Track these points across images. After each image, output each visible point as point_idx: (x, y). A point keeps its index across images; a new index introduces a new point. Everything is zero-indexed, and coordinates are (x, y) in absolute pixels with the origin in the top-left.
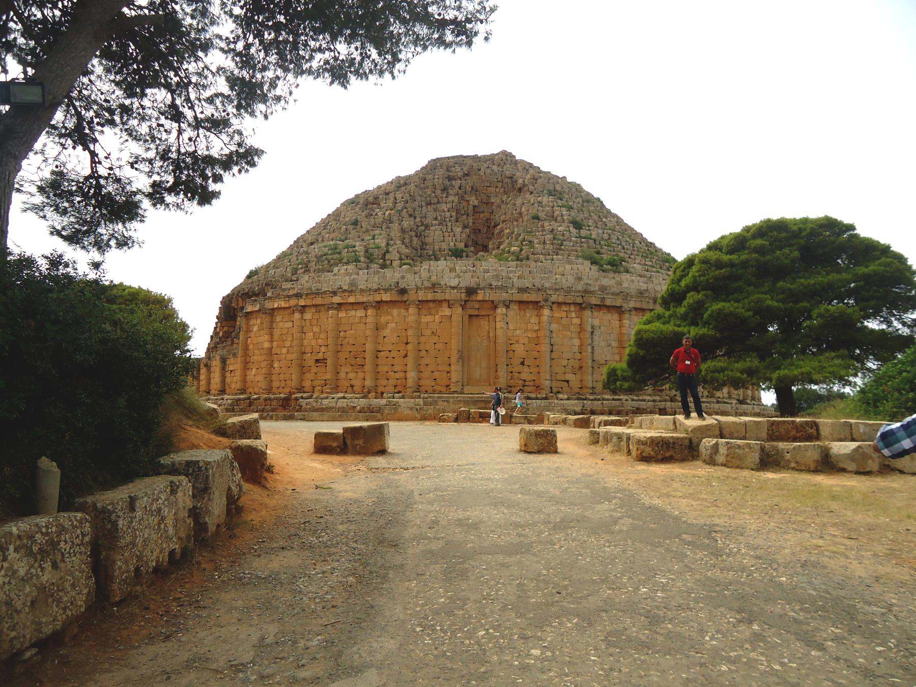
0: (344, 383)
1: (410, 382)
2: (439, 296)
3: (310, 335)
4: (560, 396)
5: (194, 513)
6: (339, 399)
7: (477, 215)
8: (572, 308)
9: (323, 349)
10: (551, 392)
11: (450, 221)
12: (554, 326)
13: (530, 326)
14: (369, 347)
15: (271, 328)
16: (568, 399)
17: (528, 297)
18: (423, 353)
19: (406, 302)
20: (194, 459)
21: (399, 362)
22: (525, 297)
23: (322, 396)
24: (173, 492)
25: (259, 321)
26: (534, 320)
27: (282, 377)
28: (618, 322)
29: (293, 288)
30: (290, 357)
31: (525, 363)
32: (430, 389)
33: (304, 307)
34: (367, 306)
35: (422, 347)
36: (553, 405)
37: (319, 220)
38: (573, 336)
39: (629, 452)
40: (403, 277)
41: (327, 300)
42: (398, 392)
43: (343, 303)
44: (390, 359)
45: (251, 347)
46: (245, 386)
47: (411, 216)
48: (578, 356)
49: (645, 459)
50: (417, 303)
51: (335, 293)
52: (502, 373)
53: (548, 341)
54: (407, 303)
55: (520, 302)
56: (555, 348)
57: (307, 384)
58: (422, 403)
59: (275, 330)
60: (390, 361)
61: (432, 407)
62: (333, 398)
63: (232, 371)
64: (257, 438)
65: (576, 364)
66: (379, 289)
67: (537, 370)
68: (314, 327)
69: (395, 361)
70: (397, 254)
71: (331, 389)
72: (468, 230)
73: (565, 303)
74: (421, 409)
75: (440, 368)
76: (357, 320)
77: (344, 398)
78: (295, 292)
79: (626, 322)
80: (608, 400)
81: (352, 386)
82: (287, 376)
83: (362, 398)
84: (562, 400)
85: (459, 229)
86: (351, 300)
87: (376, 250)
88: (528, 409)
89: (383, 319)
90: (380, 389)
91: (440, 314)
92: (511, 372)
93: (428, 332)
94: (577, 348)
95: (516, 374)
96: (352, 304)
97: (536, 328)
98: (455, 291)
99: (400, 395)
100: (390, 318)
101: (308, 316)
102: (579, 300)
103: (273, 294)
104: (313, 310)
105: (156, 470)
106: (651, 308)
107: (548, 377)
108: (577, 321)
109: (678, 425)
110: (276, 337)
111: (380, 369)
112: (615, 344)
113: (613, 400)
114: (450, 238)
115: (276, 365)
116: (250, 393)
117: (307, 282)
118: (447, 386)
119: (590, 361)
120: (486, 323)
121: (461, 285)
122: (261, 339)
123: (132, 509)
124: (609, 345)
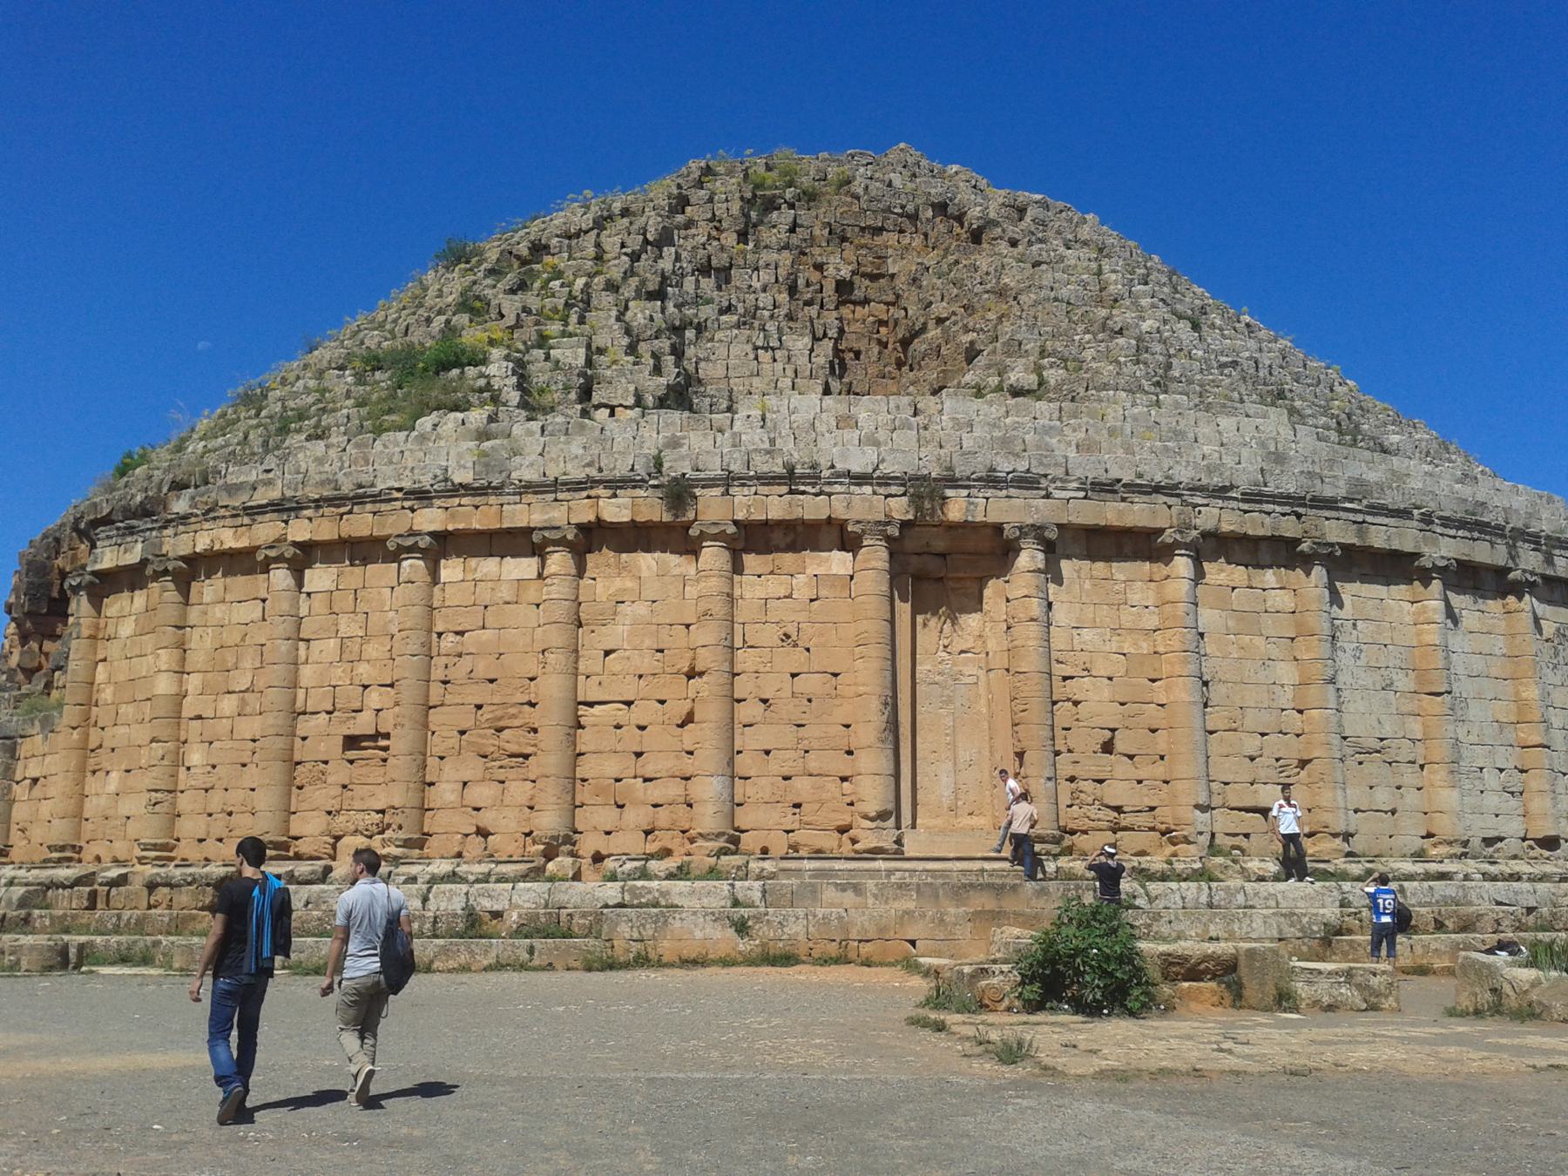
0: (448, 823)
1: (708, 818)
2: (812, 507)
7: (846, 311)
13: (1127, 617)
14: (552, 688)
17: (1120, 513)
22: (1112, 513)
27: (216, 800)
29: (269, 483)
31: (1119, 745)
32: (779, 844)
35: (742, 687)
36: (1240, 899)
38: (1275, 652)
40: (674, 443)
42: (666, 853)
44: (630, 732)
45: (107, 695)
46: (78, 836)
47: (651, 296)
50: (731, 529)
51: (421, 496)
56: (1217, 692)
61: (801, 912)
62: (413, 880)
63: (35, 781)
65: (1293, 749)
67: (1160, 770)
68: (343, 620)
69: (648, 741)
71: (407, 844)
75: (813, 761)
77: (453, 877)
78: (275, 494)
80: (1410, 877)
81: (483, 833)
82: (236, 797)
83: (524, 877)
84: (1261, 879)
90: (589, 844)
91: (810, 571)
92: (1072, 779)
93: (770, 635)
95: (1088, 786)
98: (868, 489)
100: (629, 584)
110: (196, 658)
113: (1428, 876)
114: (779, 366)
115: (196, 757)
116: (98, 859)
117: (320, 461)
118: (843, 830)
121: (886, 469)
122: (143, 666)
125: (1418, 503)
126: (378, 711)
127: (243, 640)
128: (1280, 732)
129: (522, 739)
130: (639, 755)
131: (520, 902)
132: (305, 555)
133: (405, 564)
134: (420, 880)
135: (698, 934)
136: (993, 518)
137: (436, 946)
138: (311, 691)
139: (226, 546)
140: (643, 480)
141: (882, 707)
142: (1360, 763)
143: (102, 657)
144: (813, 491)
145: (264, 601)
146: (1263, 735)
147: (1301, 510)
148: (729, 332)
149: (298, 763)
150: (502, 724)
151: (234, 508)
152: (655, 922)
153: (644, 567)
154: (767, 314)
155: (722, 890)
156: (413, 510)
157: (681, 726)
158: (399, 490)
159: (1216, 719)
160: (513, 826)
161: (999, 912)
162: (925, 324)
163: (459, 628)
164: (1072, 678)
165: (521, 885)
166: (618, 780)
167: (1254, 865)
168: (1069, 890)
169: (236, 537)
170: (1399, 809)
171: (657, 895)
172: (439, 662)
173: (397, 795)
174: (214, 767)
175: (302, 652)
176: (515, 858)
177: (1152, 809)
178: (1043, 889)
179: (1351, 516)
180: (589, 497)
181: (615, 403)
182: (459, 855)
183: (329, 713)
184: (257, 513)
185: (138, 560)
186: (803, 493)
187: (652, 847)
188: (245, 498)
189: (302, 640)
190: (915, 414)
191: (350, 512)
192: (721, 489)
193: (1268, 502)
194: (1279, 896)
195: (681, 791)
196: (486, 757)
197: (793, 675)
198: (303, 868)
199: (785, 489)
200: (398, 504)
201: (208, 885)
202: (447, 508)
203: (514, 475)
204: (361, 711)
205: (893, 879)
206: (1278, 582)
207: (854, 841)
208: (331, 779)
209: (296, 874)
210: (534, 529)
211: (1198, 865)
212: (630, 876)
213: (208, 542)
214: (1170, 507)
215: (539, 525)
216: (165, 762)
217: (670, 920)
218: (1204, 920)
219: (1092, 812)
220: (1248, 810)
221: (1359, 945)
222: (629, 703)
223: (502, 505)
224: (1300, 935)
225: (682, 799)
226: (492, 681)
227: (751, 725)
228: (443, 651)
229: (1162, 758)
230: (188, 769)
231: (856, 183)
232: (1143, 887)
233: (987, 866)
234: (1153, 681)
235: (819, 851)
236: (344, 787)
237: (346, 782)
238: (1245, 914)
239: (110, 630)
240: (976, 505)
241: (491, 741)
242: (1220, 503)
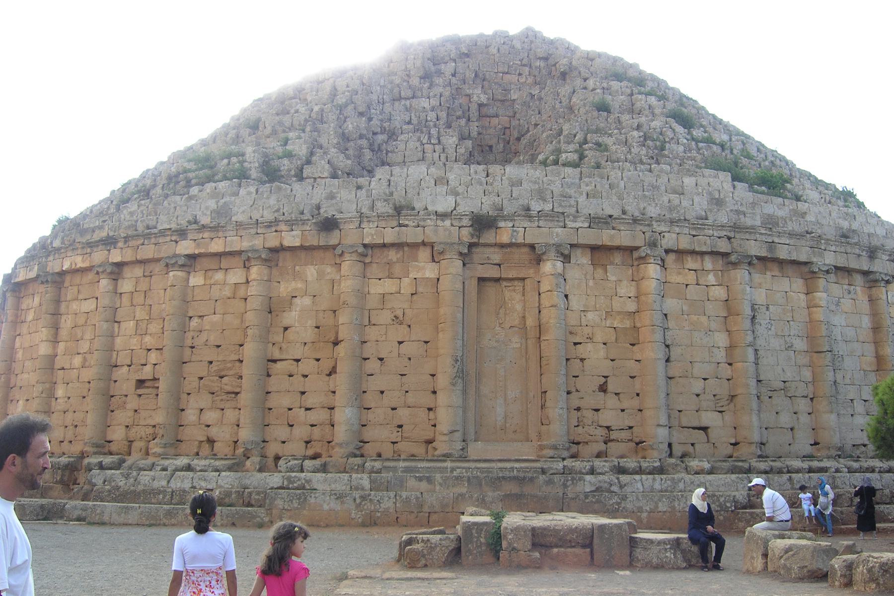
0: (193, 434)
1: (341, 433)
2: (412, 235)
3: (129, 326)
4: (694, 464)
6: (176, 470)
9: (153, 357)
10: (671, 455)
11: (435, 126)
12: (672, 304)
13: (617, 305)
14: (250, 350)
15: (56, 314)
16: (711, 472)
18: (372, 365)
19: (334, 247)
21: (317, 385)
22: (606, 237)
23: (142, 463)
25: (37, 299)
26: (626, 289)
28: (803, 297)
29: (101, 228)
30: (87, 374)
31: (610, 387)
33: (120, 265)
34: (249, 259)
35: (369, 350)
36: (681, 486)
38: (713, 326)
40: (331, 196)
41: (166, 250)
42: (315, 457)
43: (200, 255)
44: (298, 379)
45: (20, 355)
48: (727, 371)
50: (361, 250)
51: (182, 233)
52: (557, 410)
53: (658, 336)
54: (338, 251)
55: (595, 249)
56: (675, 352)
57: (117, 434)
58: (366, 483)
59: (64, 318)
60: (298, 383)
61: (392, 494)
62: (164, 469)
65: (724, 390)
66: (276, 221)
67: (636, 403)
69: (308, 385)
70: (327, 166)
72: (469, 143)
73: (693, 252)
74: (363, 498)
75: (411, 399)
76: (227, 292)
77: (189, 468)
78: (103, 234)
79: (821, 296)
80: (798, 471)
81: (211, 441)
82: (79, 416)
83: (230, 469)
85: (455, 139)
86: (216, 246)
87: (286, 161)
88: (624, 498)
89: (285, 288)
90: (273, 449)
91: (411, 276)
92: (578, 409)
93: (385, 317)
94: (723, 353)
95: (588, 414)
96: (219, 255)
97: (632, 307)
98: (447, 223)
99: (317, 462)
100: (300, 285)
101: (126, 286)
102: (723, 246)
103: (63, 243)
104: (138, 271)
106: (866, 268)
107: (663, 420)
108: (719, 293)
110: (64, 333)
111: (273, 401)
112: (800, 344)
113: (811, 470)
114: (436, 155)
115: (60, 392)
117: (132, 214)
118: (429, 442)
119: (753, 382)
120: (518, 297)
121: (460, 209)
124: (790, 347)
125: (810, 230)
126: (155, 365)
127: (86, 322)
128: (717, 378)
129: (234, 383)
130: (303, 393)
131: (222, 484)
132: (117, 270)
133: (171, 274)
134: (169, 469)
135: (326, 507)
136: (529, 241)
137: (164, 510)
138: (120, 353)
139: (78, 266)
140: (308, 220)
141: (454, 363)
142: (770, 397)
143: (18, 333)
144: (414, 224)
146: (705, 379)
147: (731, 235)
148: (406, 135)
149: (112, 396)
150: (223, 373)
151: (83, 243)
152: (299, 499)
153: (309, 274)
154: (432, 124)
155: (344, 480)
156: (177, 242)
158: (170, 229)
159: (675, 369)
160: (228, 436)
161: (521, 495)
162: (528, 128)
163: (201, 314)
164: (580, 343)
165: (224, 474)
166: (290, 409)
167: (694, 464)
168: (567, 481)
169: (83, 261)
170: (796, 427)
171: (303, 481)
172: (189, 335)
173: (159, 418)
174: (69, 398)
175: (116, 330)
176: (228, 457)
177: (631, 428)
178: (550, 480)
179: (764, 238)
180: (276, 231)
181: (316, 176)
182: (197, 454)
183: (130, 366)
184: (94, 246)
185: (35, 276)
186: (406, 226)
187: (310, 452)
188: (88, 237)
189: (117, 322)
190: (487, 176)
192: (357, 224)
193: (709, 229)
194: (708, 484)
195: (328, 417)
196: (213, 393)
197: (400, 343)
199: (395, 223)
200: (168, 239)
201: (59, 468)
202: (195, 240)
203: (234, 219)
204: (145, 365)
205: (455, 474)
206: (716, 282)
207: (435, 449)
208: (129, 406)
209: (104, 463)
210: (243, 251)
211: (657, 464)
212: (291, 470)
213: (69, 264)
214: (644, 233)
215: (245, 249)
216: (44, 395)
217: (308, 498)
218: (656, 499)
219: (591, 430)
220: (694, 428)
221: (757, 515)
222: (298, 361)
223: (226, 237)
224: (719, 509)
225: (328, 422)
226: (218, 346)
227: (372, 375)
228: (191, 329)
229: (638, 395)
230: (57, 399)
231: (492, 47)
232: (618, 479)
233: (517, 465)
234: (633, 345)
235: (413, 455)
236: (136, 411)
237: (137, 409)
238: (682, 496)
239: (23, 318)
240: (517, 232)
241: (216, 384)
242: (677, 230)
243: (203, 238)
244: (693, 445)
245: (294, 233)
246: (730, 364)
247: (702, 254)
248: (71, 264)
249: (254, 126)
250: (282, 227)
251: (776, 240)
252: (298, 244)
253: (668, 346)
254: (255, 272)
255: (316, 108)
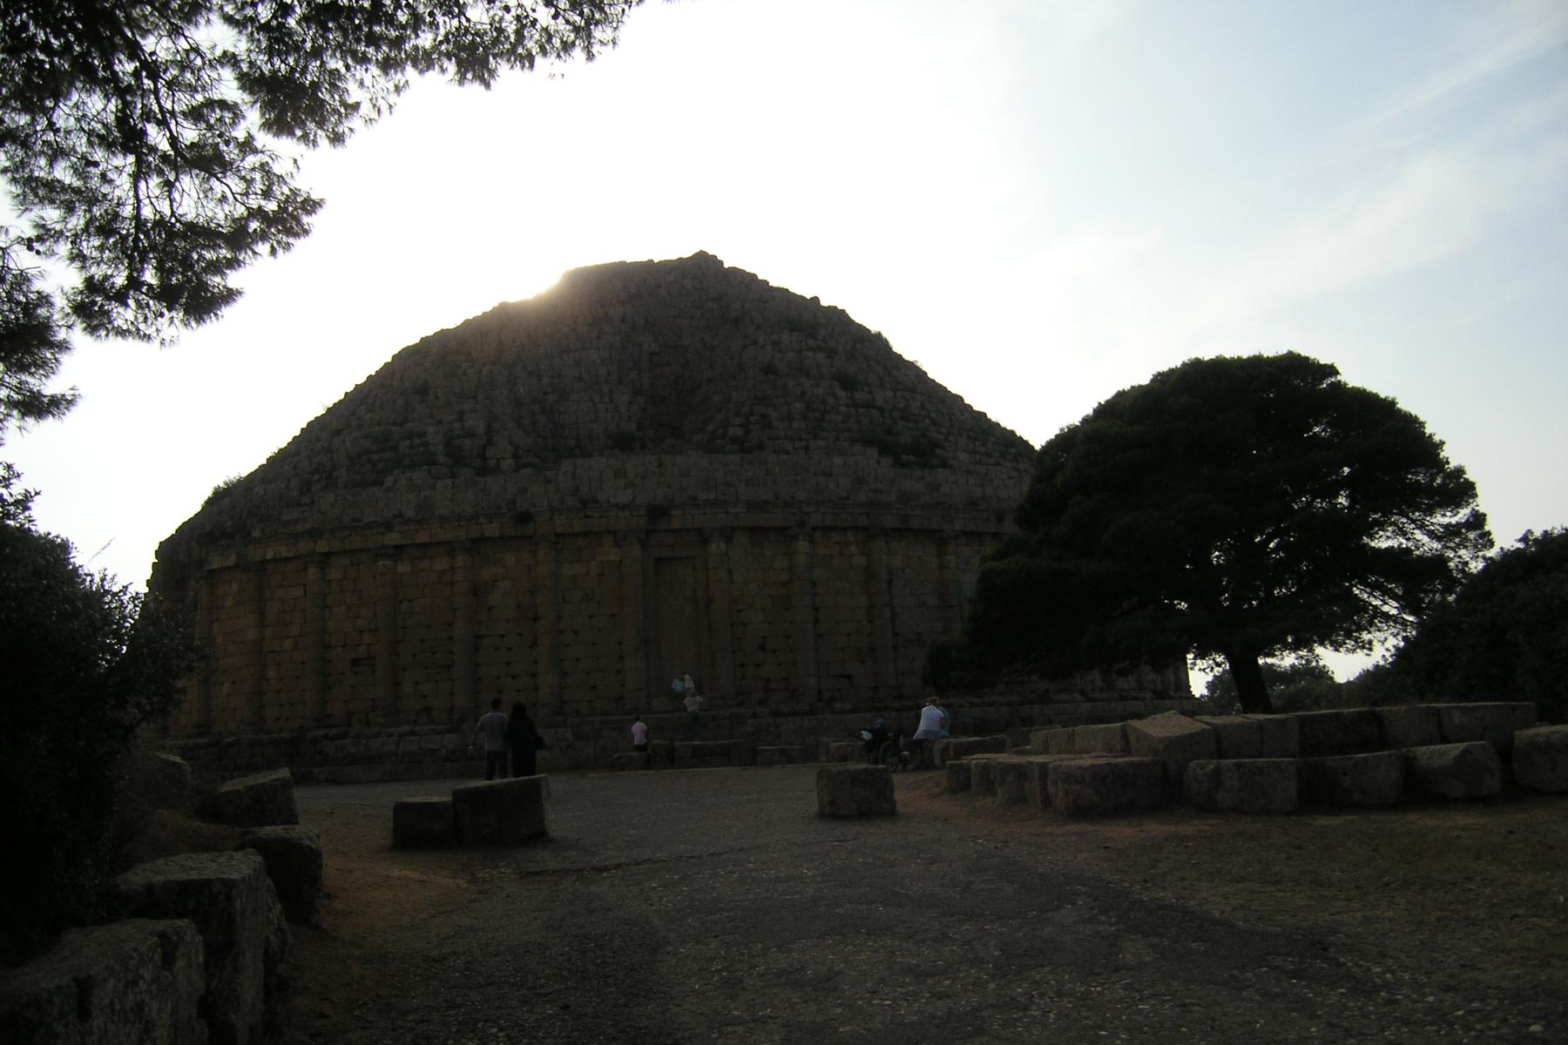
4: (838, 706)
5: (207, 1007)
6: (401, 736)
8: (851, 537)
9: (367, 638)
20: (194, 876)
24: (168, 960)
25: (235, 586)
33: (327, 555)
37: (350, 388)
39: (1047, 802)
49: (1081, 812)
51: (388, 526)
62: (391, 735)
64: (289, 822)
70: (510, 448)
77: (412, 733)
78: (308, 526)
81: (428, 709)
83: (449, 732)
86: (422, 538)
92: (742, 665)
96: (425, 546)
98: (627, 513)
101: (334, 574)
105: (118, 907)
108: (861, 561)
109: (1132, 739)
115: (271, 673)
123: (84, 1013)
130: (509, 664)
132: (324, 560)
133: (381, 563)
145: (305, 585)
154: (603, 379)
156: (383, 533)
157: (531, 647)
158: (376, 522)
166: (498, 678)
180: (477, 524)
182: (416, 721)
186: (592, 517)
191: (349, 536)
197: (591, 617)
198: (333, 732)
203: (437, 513)
222: (502, 636)
226: (429, 626)
234: (787, 609)
243: (409, 530)
244: (839, 690)
245: (493, 525)
246: (870, 621)
247: (845, 529)
248: (275, 554)
249: (423, 391)
250: (483, 520)
251: (911, 513)
252: (497, 535)
253: (816, 609)
254: (460, 560)
255: (485, 371)
